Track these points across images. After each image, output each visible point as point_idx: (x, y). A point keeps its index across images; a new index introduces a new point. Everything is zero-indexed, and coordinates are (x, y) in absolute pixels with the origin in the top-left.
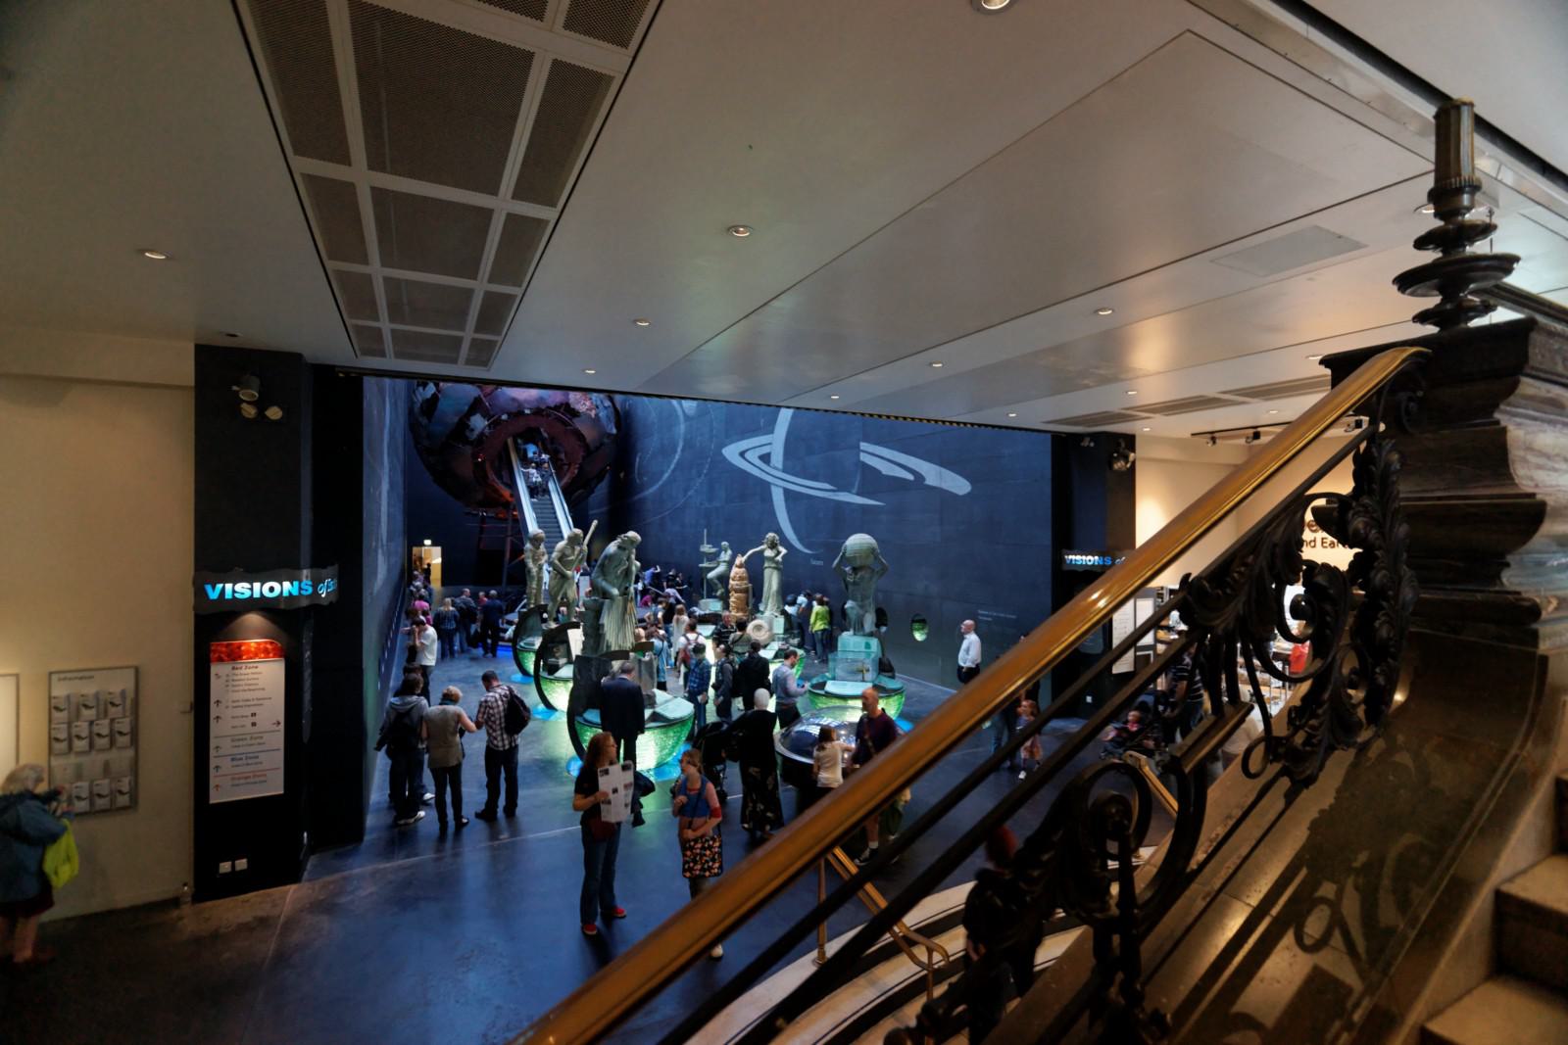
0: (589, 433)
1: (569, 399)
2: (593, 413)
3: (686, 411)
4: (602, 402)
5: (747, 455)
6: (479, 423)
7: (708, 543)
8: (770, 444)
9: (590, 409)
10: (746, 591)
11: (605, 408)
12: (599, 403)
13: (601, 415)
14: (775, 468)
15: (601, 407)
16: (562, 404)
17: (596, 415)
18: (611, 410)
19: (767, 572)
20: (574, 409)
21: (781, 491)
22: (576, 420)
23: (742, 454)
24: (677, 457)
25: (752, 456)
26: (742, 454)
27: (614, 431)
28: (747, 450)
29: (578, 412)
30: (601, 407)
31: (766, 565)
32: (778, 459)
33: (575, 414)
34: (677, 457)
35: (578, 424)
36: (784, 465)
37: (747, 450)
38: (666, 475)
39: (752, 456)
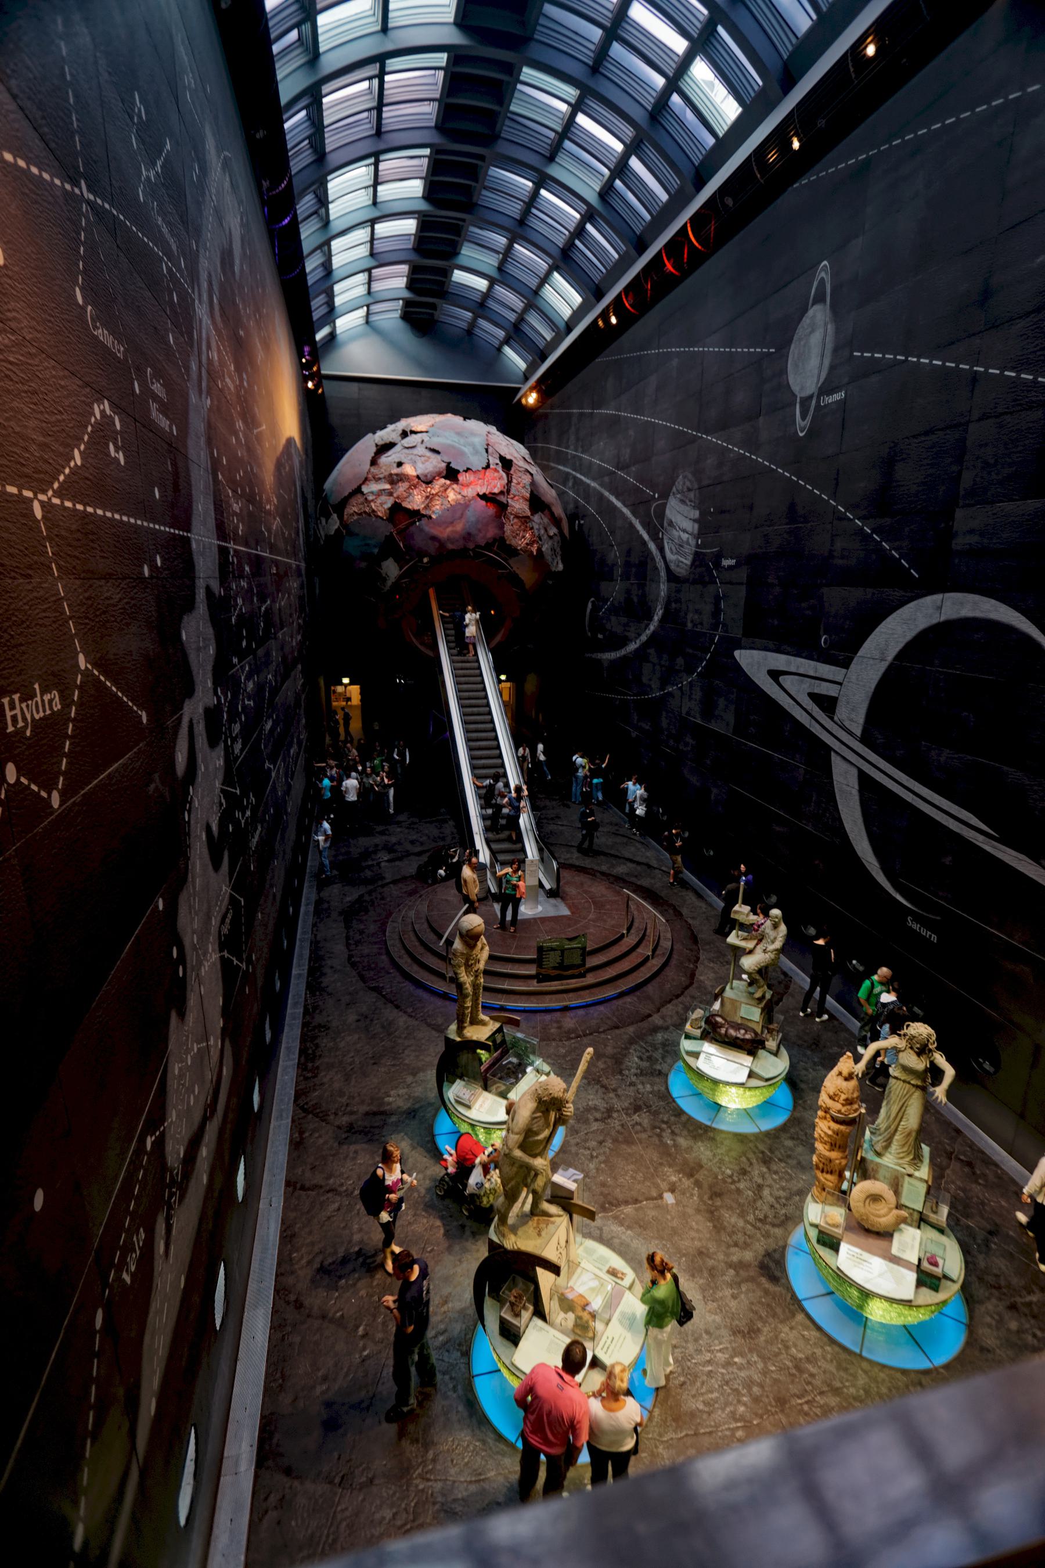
0: (527, 575)
1: (504, 533)
2: (534, 549)
3: (672, 567)
4: (546, 530)
6: (391, 569)
7: (744, 903)
9: (531, 543)
11: (551, 537)
12: (542, 532)
13: (544, 549)
15: (545, 537)
16: (495, 540)
17: (539, 550)
18: (557, 538)
20: (510, 545)
22: (512, 561)
24: (652, 628)
29: (516, 550)
33: (512, 552)
34: (652, 628)
36: (865, 731)
38: (632, 647)
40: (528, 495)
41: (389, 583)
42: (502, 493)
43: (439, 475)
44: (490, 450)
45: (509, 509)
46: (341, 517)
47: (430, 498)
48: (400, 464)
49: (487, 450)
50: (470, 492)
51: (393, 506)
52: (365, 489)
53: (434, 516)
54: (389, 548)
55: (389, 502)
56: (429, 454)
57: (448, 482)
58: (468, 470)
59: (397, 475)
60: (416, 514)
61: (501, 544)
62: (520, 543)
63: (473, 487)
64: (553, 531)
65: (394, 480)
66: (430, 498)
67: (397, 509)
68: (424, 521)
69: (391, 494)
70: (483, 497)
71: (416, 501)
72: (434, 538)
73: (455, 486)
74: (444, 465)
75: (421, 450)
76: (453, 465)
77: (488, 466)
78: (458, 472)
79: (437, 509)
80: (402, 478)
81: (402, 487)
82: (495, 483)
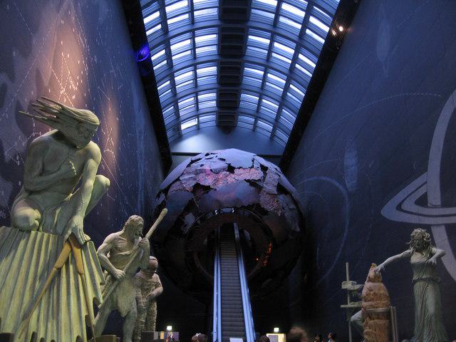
4: (287, 205)
5: (405, 207)
6: (190, 219)
7: (350, 280)
8: (426, 183)
10: (387, 315)
13: (286, 215)
14: (435, 207)
15: (287, 208)
16: (254, 204)
17: (283, 215)
19: (418, 288)
20: (264, 208)
21: (443, 227)
23: (399, 208)
25: (410, 205)
26: (399, 208)
27: (298, 229)
28: (403, 201)
30: (287, 208)
31: (415, 278)
32: (435, 197)
33: (265, 212)
35: (267, 221)
37: (403, 201)
39: (410, 205)
40: (276, 184)
41: (188, 227)
42: (259, 180)
43: (224, 170)
44: (255, 161)
45: (264, 189)
46: (166, 195)
47: (217, 180)
48: (202, 165)
49: (253, 161)
50: (242, 178)
51: (195, 185)
52: (181, 178)
53: (218, 189)
54: (190, 207)
55: (193, 183)
56: (218, 161)
57: (228, 173)
58: (239, 168)
59: (200, 170)
60: (207, 188)
61: (257, 207)
62: (268, 208)
63: (241, 175)
64: (292, 206)
65: (197, 172)
66: (217, 180)
67: (198, 186)
68: (212, 191)
69: (195, 179)
70: (248, 181)
71: (208, 181)
72: (217, 201)
73: (232, 175)
74: (227, 165)
75: (215, 159)
76: (232, 165)
77: (252, 167)
78: (234, 168)
79: (220, 185)
80: (202, 171)
81: (201, 177)
82: (256, 175)
